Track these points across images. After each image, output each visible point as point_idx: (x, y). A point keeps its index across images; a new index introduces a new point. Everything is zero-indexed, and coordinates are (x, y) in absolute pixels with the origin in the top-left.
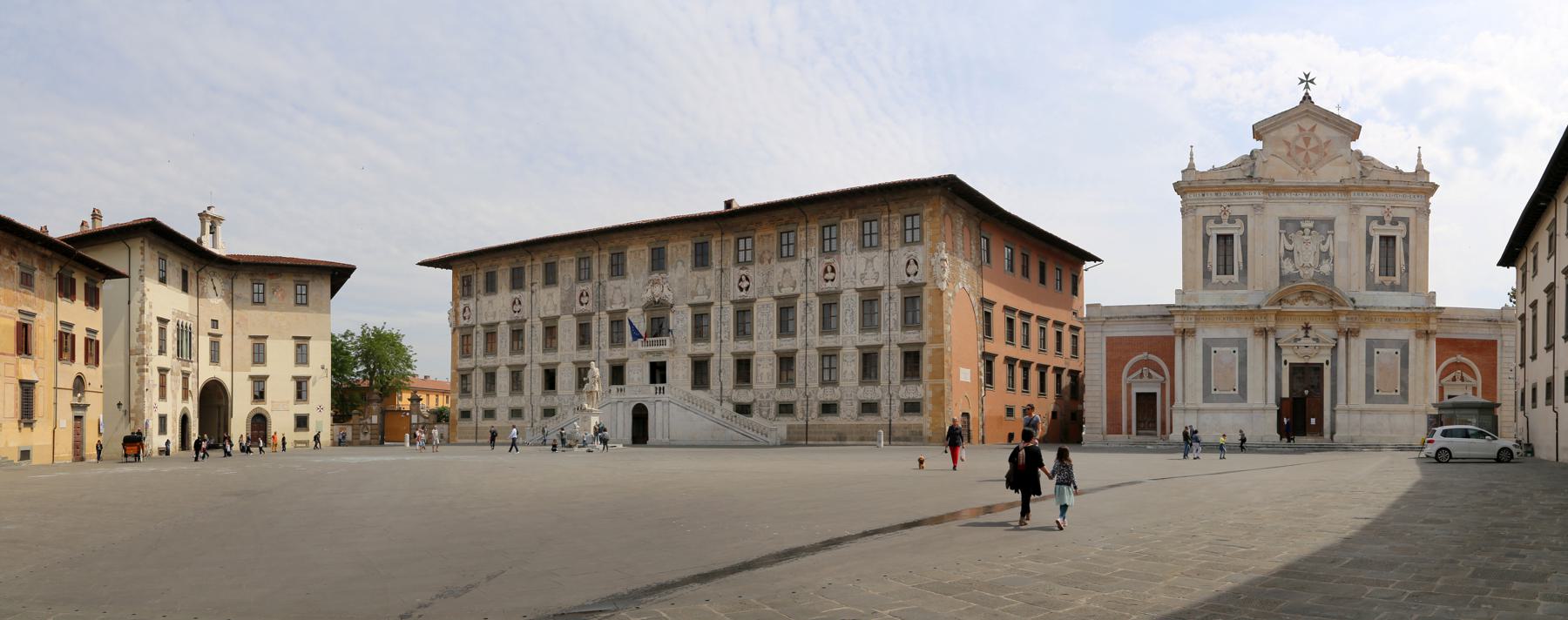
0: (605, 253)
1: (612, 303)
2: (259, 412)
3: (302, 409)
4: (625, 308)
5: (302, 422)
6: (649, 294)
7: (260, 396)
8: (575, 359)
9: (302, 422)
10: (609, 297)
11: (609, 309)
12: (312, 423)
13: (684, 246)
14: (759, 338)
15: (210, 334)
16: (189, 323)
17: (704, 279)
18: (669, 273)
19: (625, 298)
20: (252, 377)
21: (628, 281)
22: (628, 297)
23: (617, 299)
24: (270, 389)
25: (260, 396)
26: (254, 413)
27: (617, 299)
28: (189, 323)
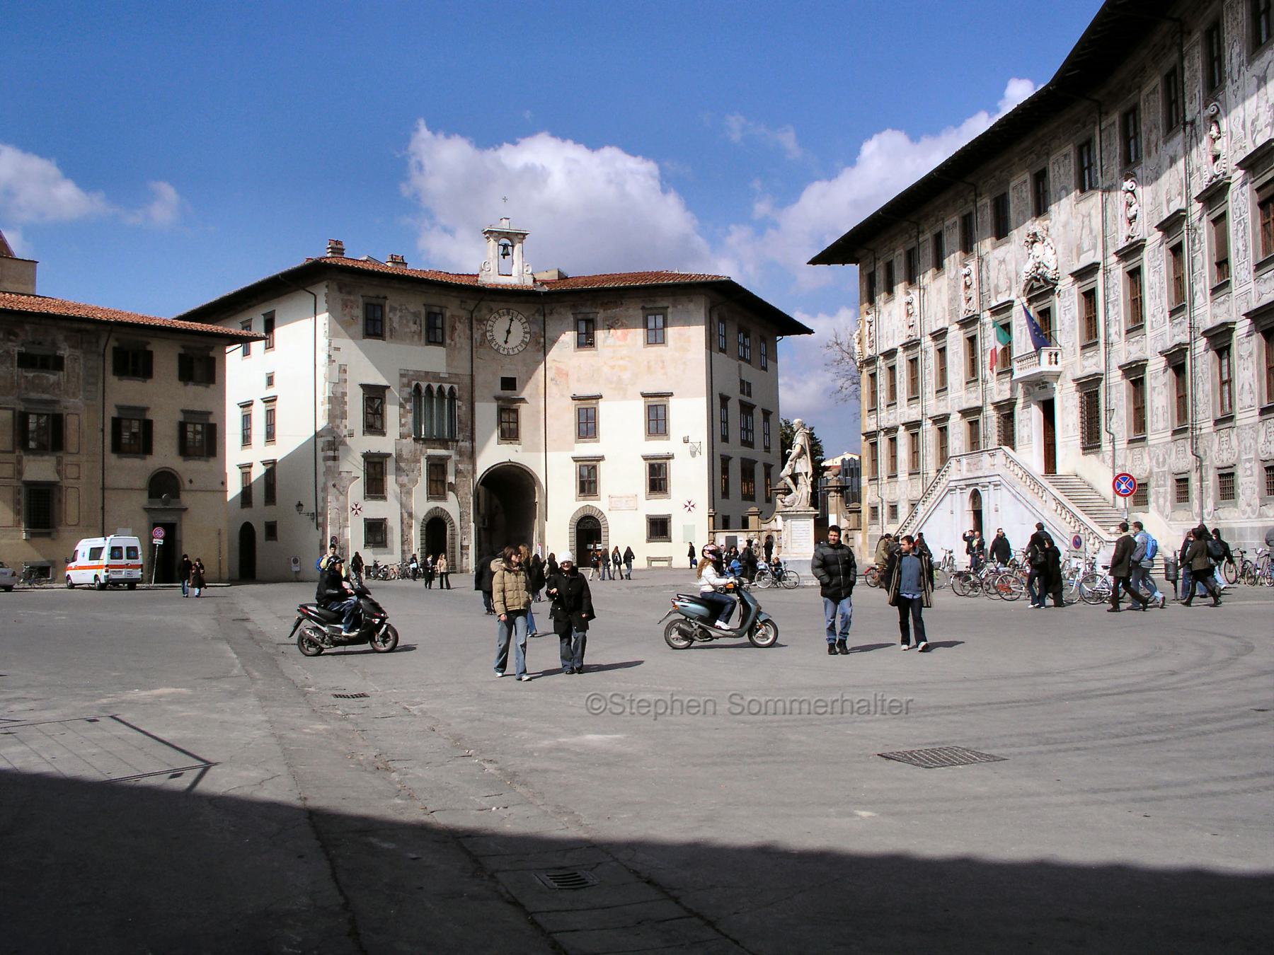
0: (984, 201)
1: (997, 293)
2: (589, 512)
3: (659, 507)
4: (1011, 298)
5: (659, 528)
6: (1029, 266)
7: (588, 484)
8: (965, 406)
9: (659, 528)
10: (993, 282)
11: (994, 304)
12: (675, 528)
13: (1065, 156)
14: (1152, 327)
15: (497, 399)
16: (447, 387)
17: (1089, 215)
18: (1052, 217)
19: (1010, 279)
20: (576, 460)
21: (1013, 246)
22: (1013, 275)
23: (1003, 285)
24: (606, 476)
25: (588, 484)
26: (581, 514)
27: (1003, 285)
28: (447, 387)
